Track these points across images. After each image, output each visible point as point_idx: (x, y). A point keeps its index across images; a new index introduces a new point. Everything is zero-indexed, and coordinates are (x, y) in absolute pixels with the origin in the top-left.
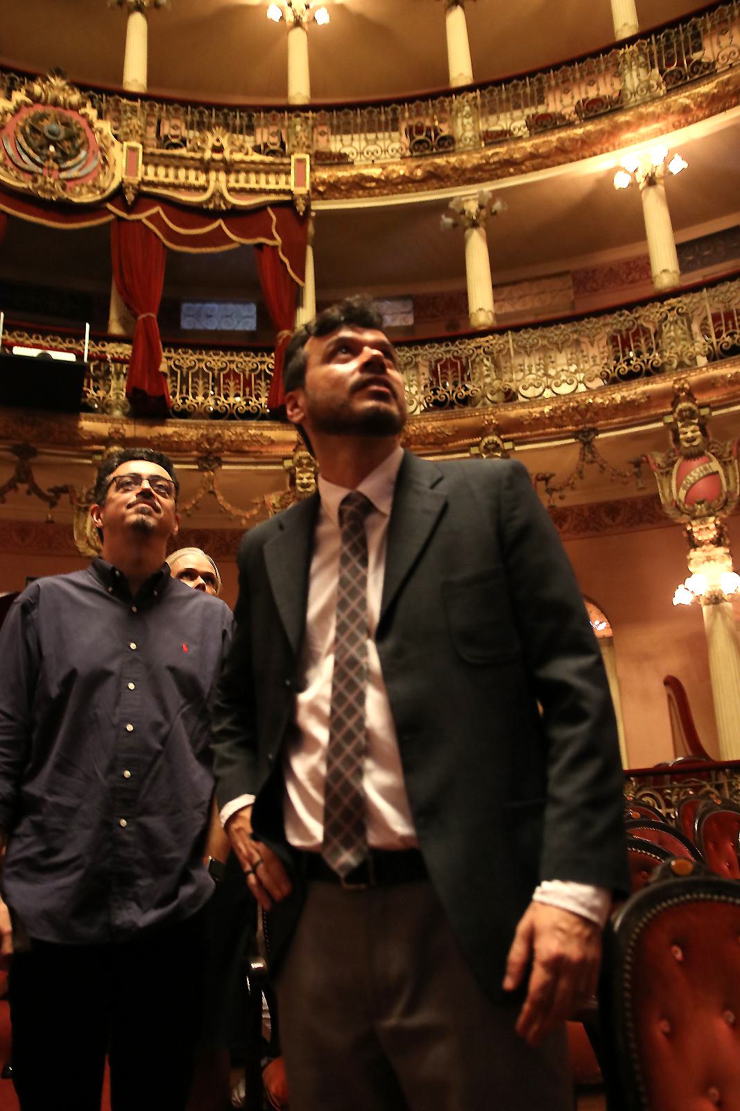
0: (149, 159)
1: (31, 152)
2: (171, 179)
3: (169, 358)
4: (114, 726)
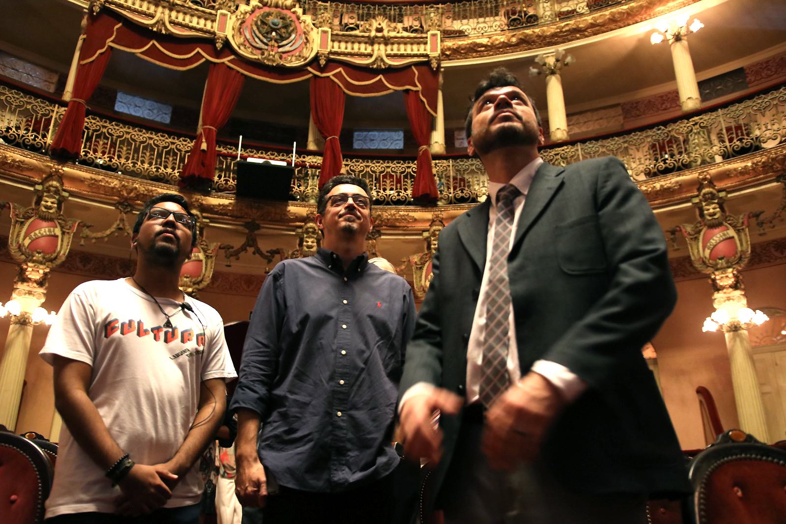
0: (335, 38)
1: (261, 36)
2: (349, 50)
3: (346, 165)
4: (333, 351)
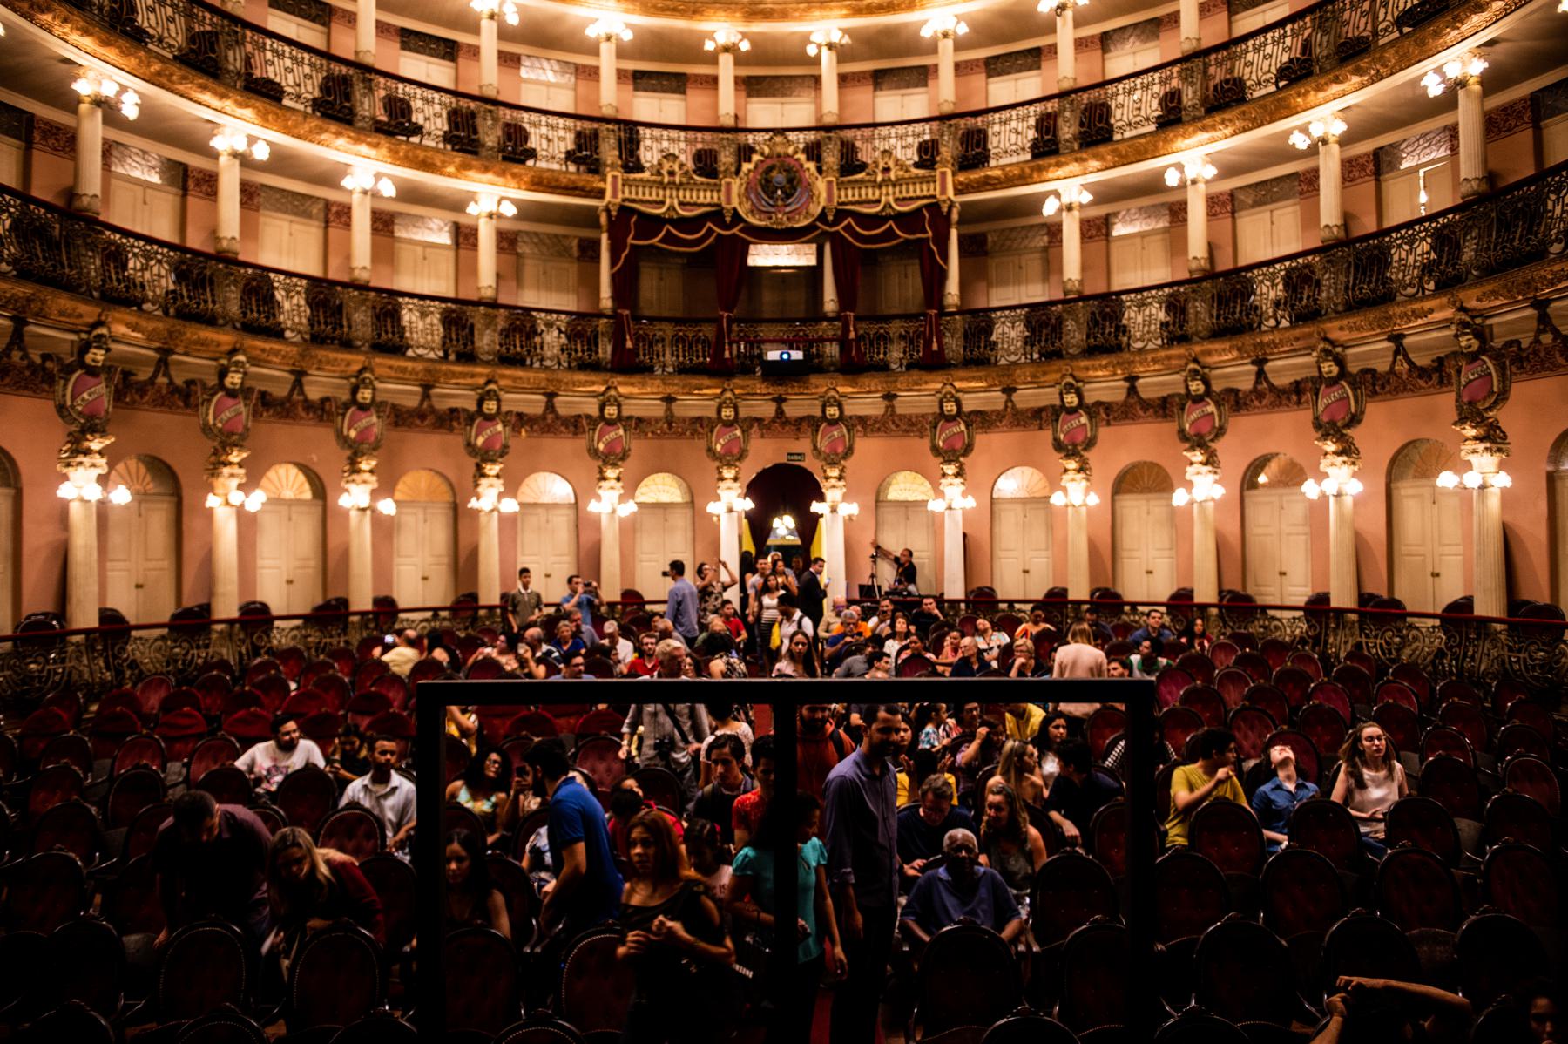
0: (840, 185)
